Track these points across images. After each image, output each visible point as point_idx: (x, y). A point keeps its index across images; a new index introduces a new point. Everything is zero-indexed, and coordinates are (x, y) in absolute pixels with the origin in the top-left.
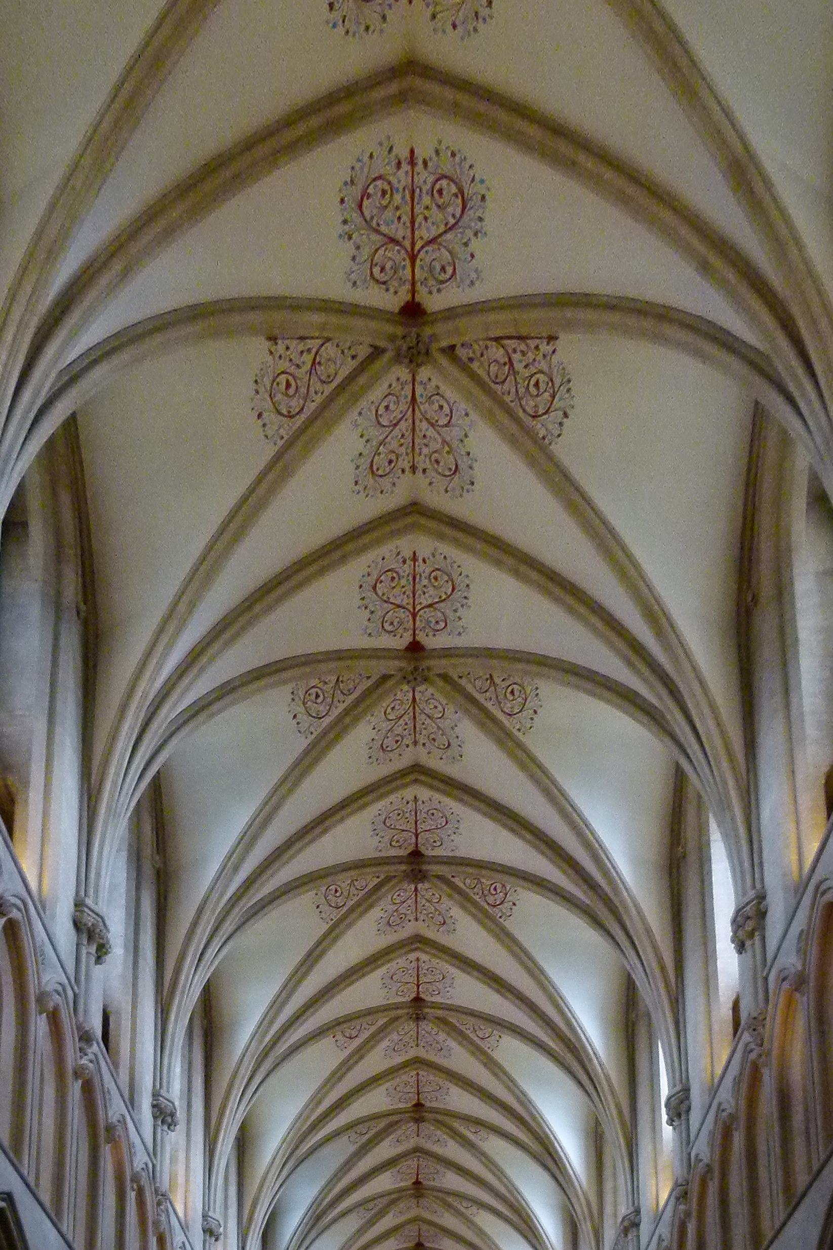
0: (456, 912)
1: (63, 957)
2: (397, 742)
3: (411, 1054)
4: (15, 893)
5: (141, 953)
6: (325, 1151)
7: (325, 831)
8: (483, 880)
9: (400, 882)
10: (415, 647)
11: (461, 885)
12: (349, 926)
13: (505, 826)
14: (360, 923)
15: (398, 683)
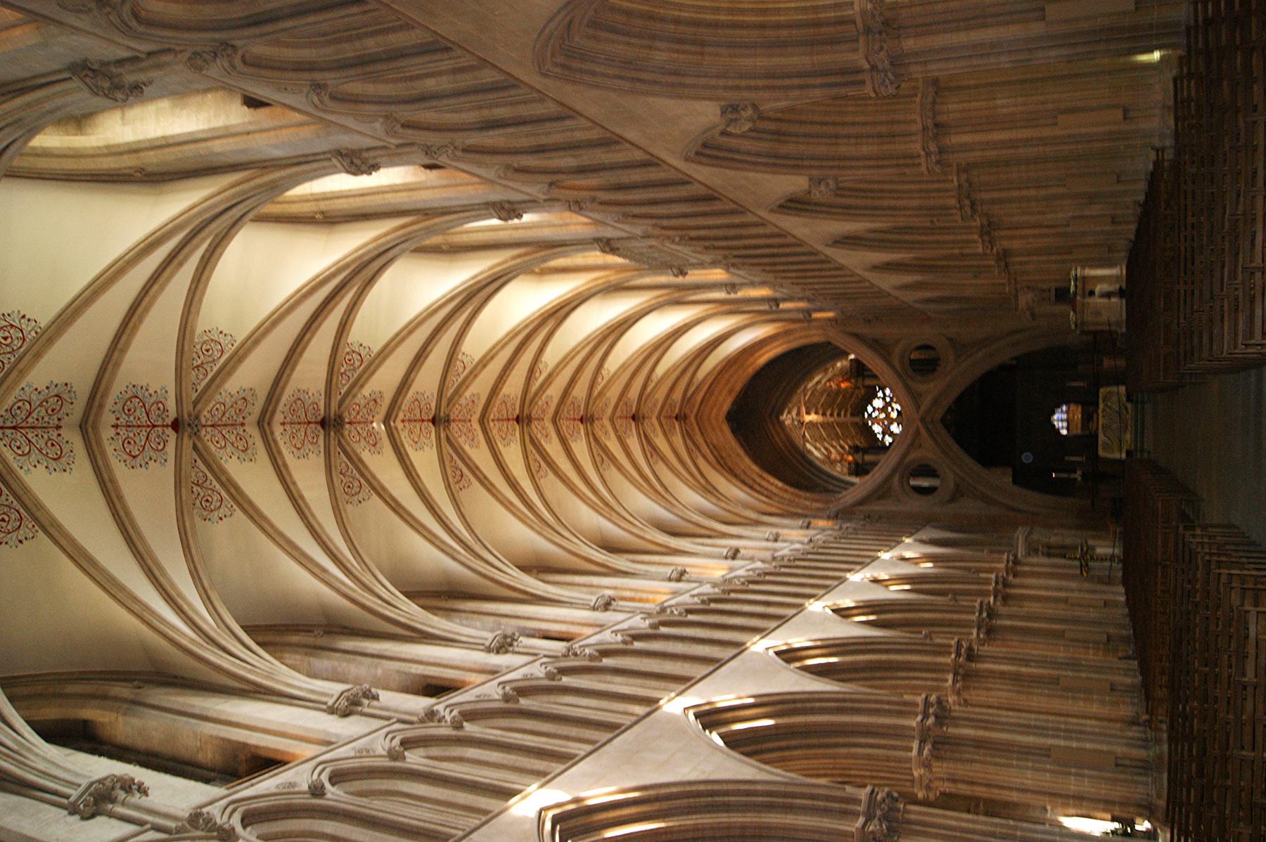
0: (366, 391)
1: (367, 730)
2: (53, 445)
3: (476, 426)
4: (310, 772)
5: (381, 653)
6: (549, 495)
7: (302, 497)
8: (343, 370)
9: (342, 435)
10: (176, 425)
11: (346, 388)
12: (374, 477)
13: (301, 354)
14: (372, 468)
15: (199, 438)
